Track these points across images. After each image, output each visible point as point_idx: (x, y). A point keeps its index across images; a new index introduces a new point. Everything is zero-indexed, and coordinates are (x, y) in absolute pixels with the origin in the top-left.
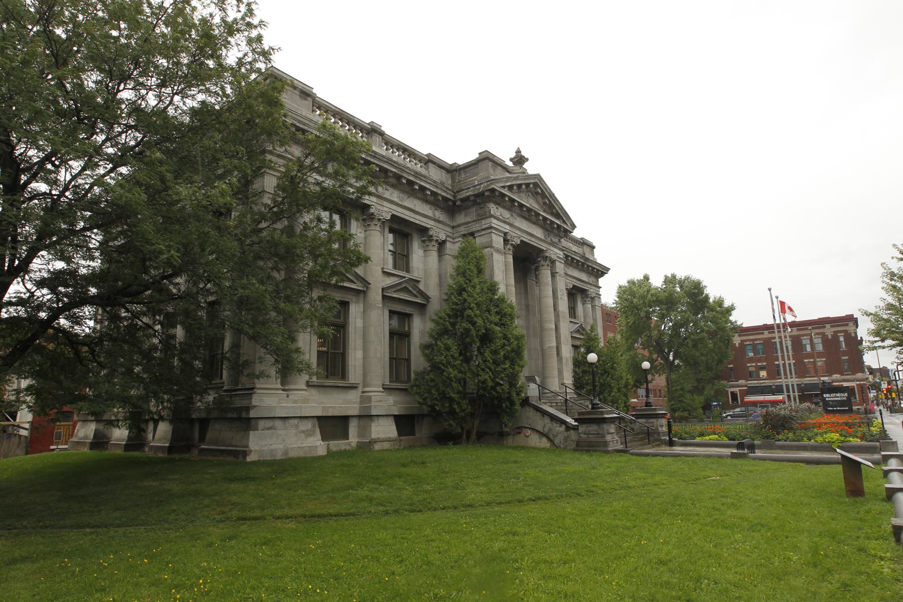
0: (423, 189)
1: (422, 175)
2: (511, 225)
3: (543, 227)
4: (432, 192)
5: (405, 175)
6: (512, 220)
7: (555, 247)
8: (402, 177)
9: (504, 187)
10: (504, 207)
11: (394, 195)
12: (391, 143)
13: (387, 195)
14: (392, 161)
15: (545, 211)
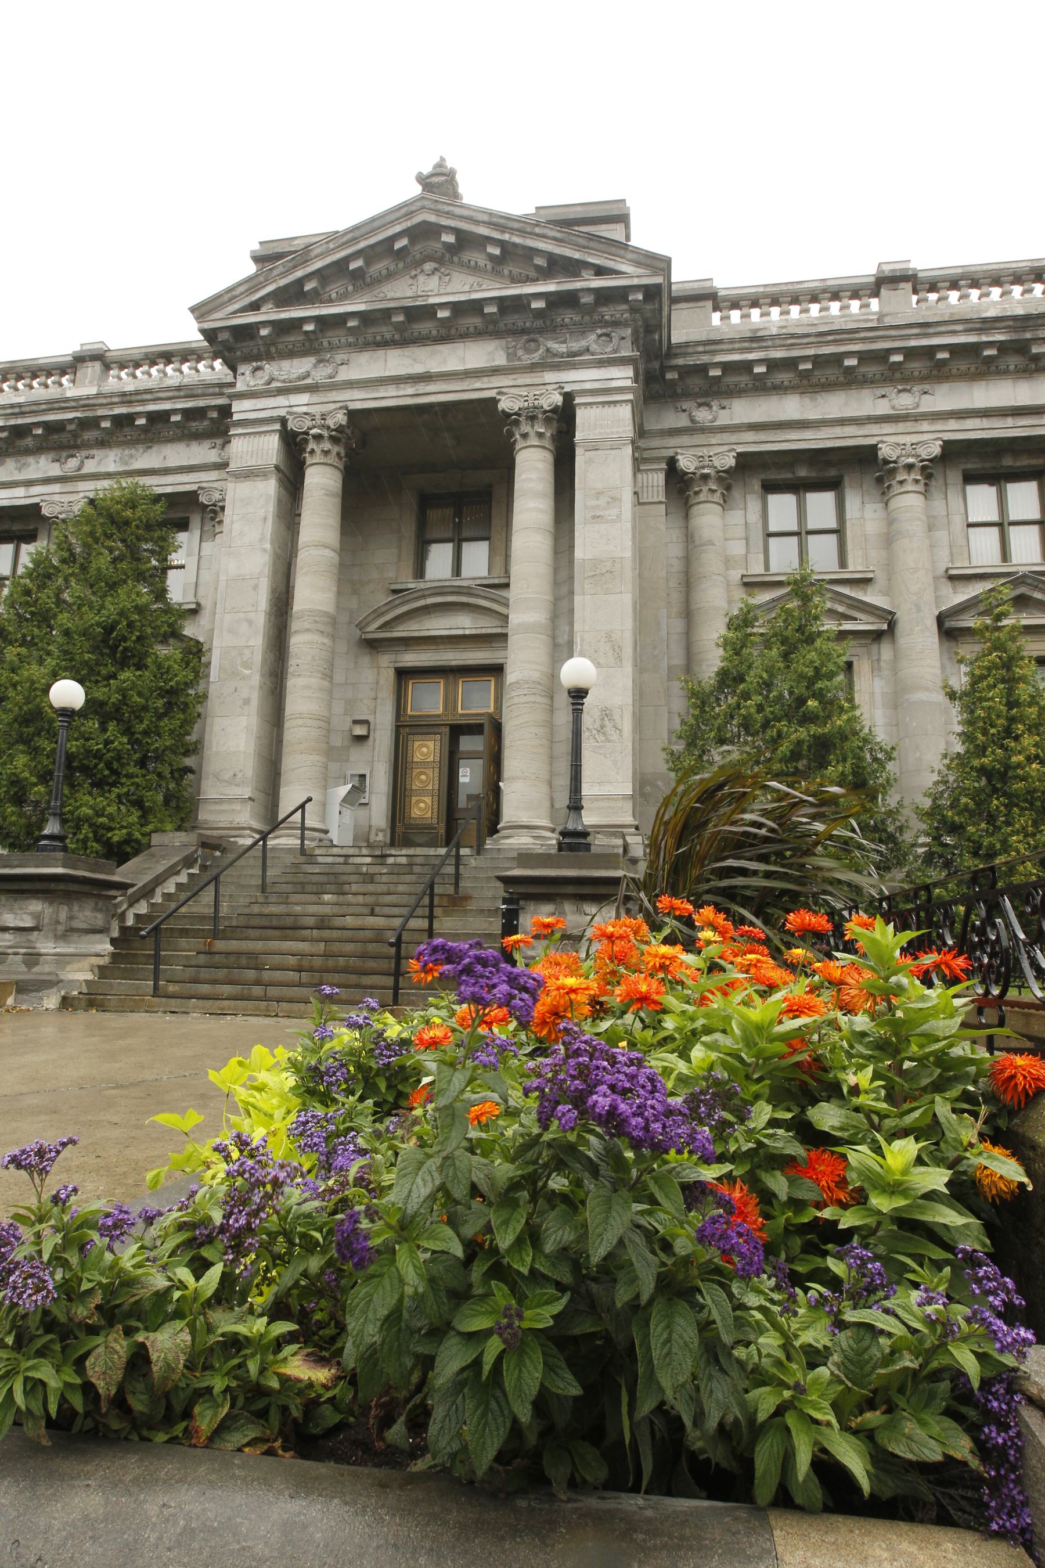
0: (158, 418)
3: (489, 330)
4: (187, 413)
5: (100, 412)
6: (320, 375)
7: (574, 366)
9: (255, 306)
10: (291, 354)
11: (109, 461)
12: (131, 362)
13: (90, 467)
14: (67, 400)
15: (515, 280)
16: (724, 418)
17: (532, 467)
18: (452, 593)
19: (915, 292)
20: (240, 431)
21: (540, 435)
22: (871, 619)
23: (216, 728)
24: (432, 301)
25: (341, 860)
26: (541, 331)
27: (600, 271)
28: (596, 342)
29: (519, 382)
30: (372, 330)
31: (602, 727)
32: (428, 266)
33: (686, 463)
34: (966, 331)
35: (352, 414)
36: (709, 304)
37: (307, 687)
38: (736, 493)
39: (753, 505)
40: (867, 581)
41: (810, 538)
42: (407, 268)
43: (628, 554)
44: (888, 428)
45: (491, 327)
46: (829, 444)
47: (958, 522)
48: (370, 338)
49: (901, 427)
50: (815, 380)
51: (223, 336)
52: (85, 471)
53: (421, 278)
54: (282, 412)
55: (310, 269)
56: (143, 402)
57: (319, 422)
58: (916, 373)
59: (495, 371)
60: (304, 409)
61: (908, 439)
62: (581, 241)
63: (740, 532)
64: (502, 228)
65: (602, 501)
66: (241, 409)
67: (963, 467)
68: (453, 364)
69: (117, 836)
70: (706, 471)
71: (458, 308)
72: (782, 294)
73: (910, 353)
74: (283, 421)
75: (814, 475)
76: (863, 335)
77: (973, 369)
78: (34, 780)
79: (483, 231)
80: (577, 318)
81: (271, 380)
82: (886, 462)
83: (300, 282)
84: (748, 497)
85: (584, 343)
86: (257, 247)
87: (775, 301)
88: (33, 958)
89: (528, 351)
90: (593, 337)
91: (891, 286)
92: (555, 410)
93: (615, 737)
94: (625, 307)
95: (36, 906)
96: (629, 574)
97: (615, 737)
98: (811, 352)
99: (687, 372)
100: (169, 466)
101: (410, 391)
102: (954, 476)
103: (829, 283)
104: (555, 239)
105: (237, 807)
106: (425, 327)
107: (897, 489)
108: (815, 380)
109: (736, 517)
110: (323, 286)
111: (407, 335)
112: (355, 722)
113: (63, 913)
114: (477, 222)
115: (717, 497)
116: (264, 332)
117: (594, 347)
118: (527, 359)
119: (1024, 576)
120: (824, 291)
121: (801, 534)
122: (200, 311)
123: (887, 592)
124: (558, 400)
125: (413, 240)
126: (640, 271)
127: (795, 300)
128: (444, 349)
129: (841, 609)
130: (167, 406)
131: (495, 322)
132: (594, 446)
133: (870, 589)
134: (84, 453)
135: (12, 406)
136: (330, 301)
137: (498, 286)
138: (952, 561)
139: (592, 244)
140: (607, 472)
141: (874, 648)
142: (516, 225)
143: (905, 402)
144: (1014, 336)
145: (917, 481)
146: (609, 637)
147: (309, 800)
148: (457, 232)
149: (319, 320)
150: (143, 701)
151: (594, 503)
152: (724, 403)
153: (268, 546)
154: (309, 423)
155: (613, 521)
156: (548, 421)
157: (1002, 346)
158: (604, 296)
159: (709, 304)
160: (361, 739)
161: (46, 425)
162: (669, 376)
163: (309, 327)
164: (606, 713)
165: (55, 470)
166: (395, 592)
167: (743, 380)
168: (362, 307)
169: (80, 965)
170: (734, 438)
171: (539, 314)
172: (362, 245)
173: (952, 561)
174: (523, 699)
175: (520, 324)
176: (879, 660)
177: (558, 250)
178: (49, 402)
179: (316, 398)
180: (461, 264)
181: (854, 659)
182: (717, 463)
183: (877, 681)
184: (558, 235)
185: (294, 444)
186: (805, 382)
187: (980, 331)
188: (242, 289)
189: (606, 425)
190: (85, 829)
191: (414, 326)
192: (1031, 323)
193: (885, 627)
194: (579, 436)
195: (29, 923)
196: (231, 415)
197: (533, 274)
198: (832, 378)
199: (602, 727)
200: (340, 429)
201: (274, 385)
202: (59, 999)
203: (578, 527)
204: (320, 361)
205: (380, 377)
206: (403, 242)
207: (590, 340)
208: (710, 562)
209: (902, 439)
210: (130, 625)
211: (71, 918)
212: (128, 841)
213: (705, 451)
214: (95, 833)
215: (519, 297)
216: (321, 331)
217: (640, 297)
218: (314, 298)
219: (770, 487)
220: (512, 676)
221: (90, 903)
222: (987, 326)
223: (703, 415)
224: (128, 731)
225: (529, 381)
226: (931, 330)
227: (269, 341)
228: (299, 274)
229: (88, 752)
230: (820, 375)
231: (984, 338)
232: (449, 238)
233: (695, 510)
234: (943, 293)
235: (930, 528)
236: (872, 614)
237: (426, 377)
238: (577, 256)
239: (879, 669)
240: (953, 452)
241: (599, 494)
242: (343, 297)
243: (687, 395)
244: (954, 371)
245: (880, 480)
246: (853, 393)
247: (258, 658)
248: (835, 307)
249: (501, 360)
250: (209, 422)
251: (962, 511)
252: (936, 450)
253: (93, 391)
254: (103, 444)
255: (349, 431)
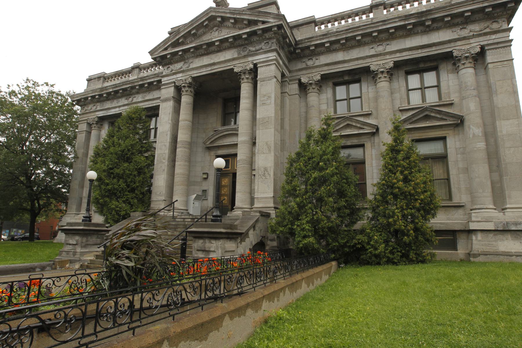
1: (145, 77)
2: (183, 72)
3: (232, 46)
5: (136, 84)
6: (184, 68)
8: (135, 86)
9: (166, 49)
10: (177, 62)
11: (139, 98)
13: (135, 100)
15: (240, 29)
16: (317, 63)
17: (245, 89)
18: (231, 130)
19: (385, 8)
20: (164, 87)
21: (247, 78)
22: (370, 128)
23: (156, 179)
24: (213, 40)
25: (182, 220)
26: (247, 44)
27: (264, 22)
28: (264, 45)
29: (241, 62)
30: (198, 51)
31: (264, 174)
32: (215, 29)
33: (304, 80)
34: (399, 21)
35: (194, 79)
36: (313, 25)
37: (180, 165)
38: (324, 88)
39: (330, 91)
40: (370, 114)
41: (351, 100)
42: (209, 30)
43: (273, 115)
44: (374, 59)
45: (232, 45)
46: (353, 67)
47: (403, 89)
48: (198, 54)
49: (379, 58)
50: (347, 46)
51: (158, 59)
52: (133, 101)
53: (213, 33)
54: (174, 80)
55: (180, 36)
56: (146, 80)
57: (185, 82)
58: (384, 38)
59: (234, 59)
60: (181, 78)
61: (381, 62)
62: (257, 14)
63: (325, 101)
64: (234, 14)
65: (265, 98)
66: (164, 80)
67: (405, 69)
68: (222, 59)
69: (123, 213)
70: (310, 82)
71: (222, 41)
72: (338, 17)
73: (380, 32)
74: (175, 83)
75: (350, 78)
76: (361, 28)
77: (405, 34)
78: (100, 198)
79: (228, 15)
80: (258, 39)
81: (172, 70)
82: (374, 71)
83: (178, 39)
84: (328, 89)
85: (260, 46)
86: (170, 30)
87: (336, 20)
88: (75, 253)
89: (244, 51)
90: (263, 44)
91: (376, 8)
92: (251, 70)
93: (268, 177)
94: (272, 33)
95: (77, 238)
96: (273, 122)
97: (268, 177)
98: (344, 36)
99: (302, 49)
100: (143, 101)
101: (210, 69)
102: (402, 73)
103: (354, 11)
104: (249, 14)
105: (161, 203)
106: (212, 48)
107: (378, 80)
108: (347, 46)
109: (324, 96)
110: (185, 40)
111: (208, 51)
112: (204, 174)
113: (84, 240)
114: (227, 13)
115: (316, 90)
116: (168, 57)
117: (264, 47)
118: (243, 54)
119: (426, 108)
120: (352, 14)
121: (349, 99)
122: (151, 53)
123: (377, 118)
124: (252, 66)
125: (210, 22)
126: (275, 20)
127: (343, 18)
128: (219, 54)
129: (359, 125)
130: (152, 80)
131: (233, 44)
132: (263, 80)
133: (371, 117)
134: (133, 96)
135: (114, 85)
136: (188, 44)
137: (235, 31)
138: (401, 105)
139: (260, 14)
140: (268, 88)
141: (372, 138)
142: (237, 12)
143: (380, 49)
144: (418, 20)
145: (385, 77)
146: (267, 143)
147: (177, 201)
148: (222, 17)
149: (183, 50)
150: (130, 172)
151: (263, 99)
152: (317, 58)
153: (170, 122)
154: (182, 83)
155: (269, 104)
156: (250, 73)
157: (414, 25)
158: (265, 30)
159: (313, 25)
160: (206, 179)
161: (123, 89)
162: (297, 51)
163: (180, 53)
164: (266, 169)
165: (126, 102)
166: (215, 131)
167: (322, 49)
168: (194, 45)
169: (90, 255)
170: (320, 69)
171: (246, 39)
172: (194, 26)
173: (401, 105)
174: (240, 166)
175: (241, 43)
176: (374, 143)
177: (250, 18)
178: (123, 83)
179: (184, 75)
180: (224, 26)
181: (365, 143)
182: (315, 79)
183: (373, 150)
184: (250, 13)
185: (178, 90)
186: (344, 47)
187: (405, 20)
188: (162, 44)
189: (269, 73)
190: (113, 212)
191: (209, 49)
192: (424, 14)
193: (375, 131)
194: (259, 77)
195: (75, 243)
196: (161, 82)
197: (245, 26)
198: (353, 44)
199: (264, 174)
200: (190, 83)
201: (173, 72)
202: (80, 265)
203: (258, 108)
204: (185, 63)
205: (202, 66)
206: (207, 23)
207: (262, 45)
208: (314, 113)
209: (379, 63)
210: (129, 150)
211: (87, 241)
212: (127, 214)
213: (311, 75)
214: (117, 214)
215: (239, 35)
216: (185, 53)
217: (276, 29)
218: (183, 44)
219: (336, 84)
220: (239, 158)
221: (96, 236)
222: (407, 18)
223: (310, 63)
224: (126, 182)
225: (244, 61)
226: (386, 23)
227: (171, 59)
228: (177, 37)
229: (114, 189)
230: (349, 44)
231: (407, 22)
232: (219, 19)
233: (308, 95)
234: (396, 7)
235: (392, 93)
236: (370, 126)
237: (214, 64)
238: (256, 19)
239: (374, 146)
240: (398, 65)
241: (264, 96)
242: (191, 42)
243: (305, 56)
244: (398, 35)
245: (373, 77)
246: (362, 48)
247: (167, 157)
248: (357, 19)
249: (236, 56)
250: (155, 85)
251: (405, 85)
252: (391, 65)
253: (136, 77)
254: (138, 93)
255: (194, 83)
